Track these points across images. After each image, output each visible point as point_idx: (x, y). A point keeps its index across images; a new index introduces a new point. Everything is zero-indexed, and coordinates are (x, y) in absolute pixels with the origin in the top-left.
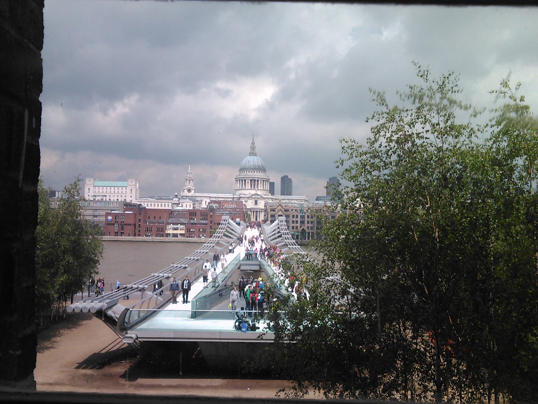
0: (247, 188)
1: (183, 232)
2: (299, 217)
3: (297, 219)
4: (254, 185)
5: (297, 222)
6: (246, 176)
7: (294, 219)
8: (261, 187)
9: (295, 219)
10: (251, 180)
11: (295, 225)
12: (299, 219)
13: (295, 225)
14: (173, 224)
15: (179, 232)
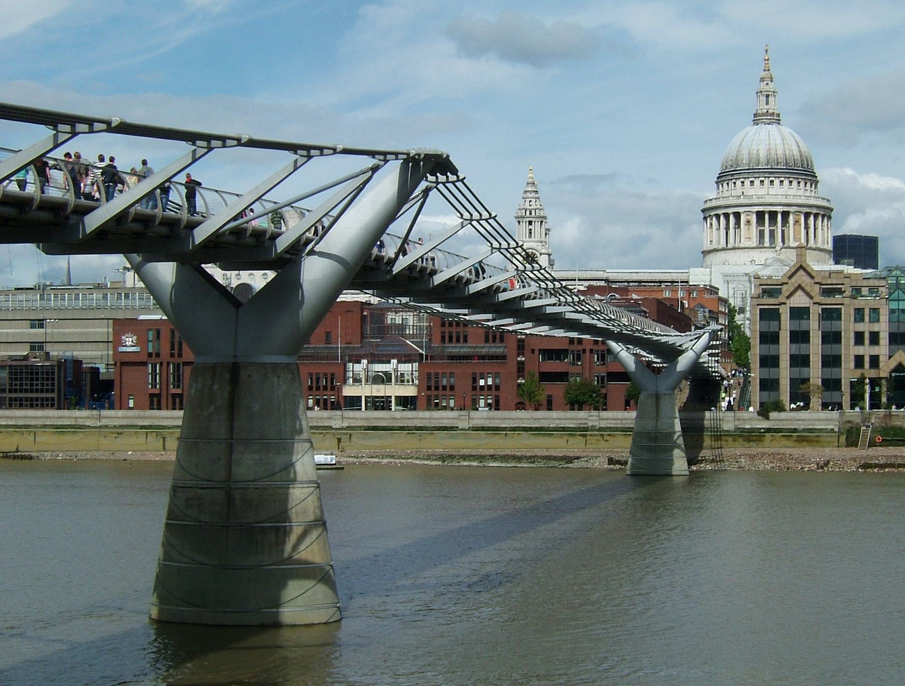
0: (744, 243)
1: (410, 391)
2: (882, 318)
3: (876, 328)
4: (772, 234)
5: (875, 338)
6: (743, 201)
7: (860, 327)
8: (795, 239)
9: (865, 327)
10: (760, 215)
11: (866, 350)
12: (883, 328)
13: (866, 350)
14: (374, 359)
15: (393, 391)
